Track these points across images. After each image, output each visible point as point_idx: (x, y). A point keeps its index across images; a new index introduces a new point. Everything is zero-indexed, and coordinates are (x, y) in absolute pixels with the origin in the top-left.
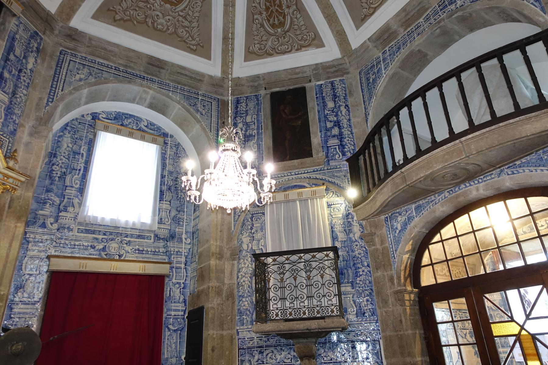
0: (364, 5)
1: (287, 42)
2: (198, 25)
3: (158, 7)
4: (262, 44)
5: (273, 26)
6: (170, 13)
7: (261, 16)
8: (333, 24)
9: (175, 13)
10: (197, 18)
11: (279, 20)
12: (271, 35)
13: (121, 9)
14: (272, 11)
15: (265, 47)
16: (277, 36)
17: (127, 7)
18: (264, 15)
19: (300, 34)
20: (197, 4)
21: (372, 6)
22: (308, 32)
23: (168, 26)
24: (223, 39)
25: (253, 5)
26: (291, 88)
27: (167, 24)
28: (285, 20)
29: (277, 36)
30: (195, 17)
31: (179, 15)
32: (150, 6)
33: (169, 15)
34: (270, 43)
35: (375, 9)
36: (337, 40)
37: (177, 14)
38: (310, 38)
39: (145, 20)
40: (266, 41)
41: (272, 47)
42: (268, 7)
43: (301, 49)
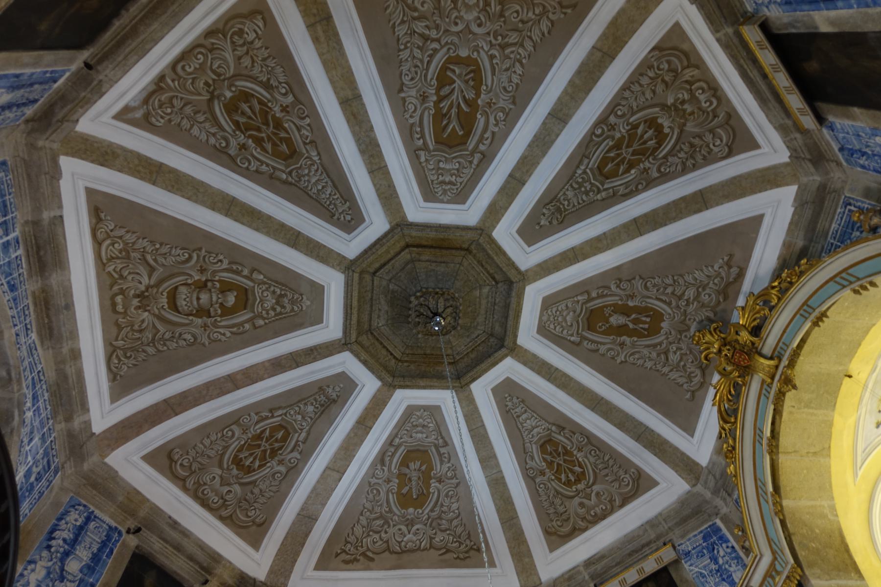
0: (122, 232)
1: (194, 79)
2: (394, 33)
3: (481, 43)
4: (242, 46)
5: (246, 96)
6: (456, 40)
7: (281, 105)
8: (136, 162)
9: (447, 43)
10: (402, 47)
11: (243, 113)
12: (237, 76)
13: (551, 15)
14: (267, 124)
15: (233, 43)
16: (224, 80)
17: (539, 22)
18: (277, 109)
19: (181, 109)
20: (410, 77)
21: (108, 242)
22: (170, 121)
23: (455, 8)
24: (331, 17)
25: (308, 121)
26: (117, 24)
27: (459, 12)
28: (231, 120)
29: (224, 80)
30: (406, 48)
31: (438, 40)
32: (496, 39)
33: (458, 33)
34: (227, 55)
35: (97, 243)
36: (101, 141)
37: (443, 43)
38: (157, 113)
39: (503, 7)
40: (240, 58)
41: (218, 52)
42: (279, 130)
43: (157, 84)
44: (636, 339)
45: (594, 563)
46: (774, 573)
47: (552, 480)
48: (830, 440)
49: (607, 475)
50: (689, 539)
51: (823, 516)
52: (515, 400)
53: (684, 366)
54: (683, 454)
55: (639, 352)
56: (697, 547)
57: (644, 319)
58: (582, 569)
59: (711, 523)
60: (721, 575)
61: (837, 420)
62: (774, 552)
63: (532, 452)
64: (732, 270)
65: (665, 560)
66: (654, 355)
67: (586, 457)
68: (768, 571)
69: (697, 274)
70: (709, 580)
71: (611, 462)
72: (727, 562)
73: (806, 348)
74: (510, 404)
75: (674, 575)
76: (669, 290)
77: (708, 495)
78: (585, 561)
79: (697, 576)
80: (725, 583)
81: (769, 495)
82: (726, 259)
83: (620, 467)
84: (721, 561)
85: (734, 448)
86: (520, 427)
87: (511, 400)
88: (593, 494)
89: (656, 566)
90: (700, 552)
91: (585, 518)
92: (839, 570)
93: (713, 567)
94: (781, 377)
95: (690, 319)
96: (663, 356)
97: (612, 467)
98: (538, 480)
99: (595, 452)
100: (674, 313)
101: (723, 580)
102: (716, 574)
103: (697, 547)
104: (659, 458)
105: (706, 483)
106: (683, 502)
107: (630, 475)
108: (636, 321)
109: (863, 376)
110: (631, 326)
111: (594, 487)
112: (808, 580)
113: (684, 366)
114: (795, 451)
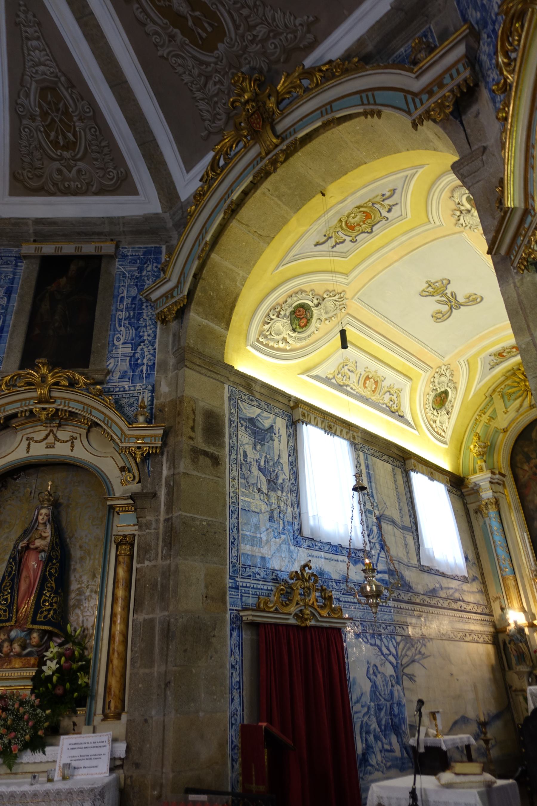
44: (187, 41)
45: (44, 224)
46: (169, 296)
47: (40, 131)
48: (277, 233)
49: (96, 160)
50: (134, 248)
51: (234, 280)
52: (30, 16)
53: (216, 103)
54: (172, 182)
55: (184, 58)
56: (135, 255)
57: (206, 25)
58: (30, 222)
59: (158, 246)
60: (137, 282)
61: (293, 221)
62: (179, 282)
63: (29, 89)
64: (308, 36)
65: (103, 251)
66: (196, 72)
67: (84, 131)
68: (167, 292)
69: (279, 15)
70: (126, 281)
71: (106, 150)
72: (147, 276)
73: (309, 147)
74: (22, 16)
75: (103, 265)
76: (245, 12)
77: (170, 224)
78: (37, 219)
79: (120, 275)
80: (136, 288)
81: (204, 242)
82: (311, 19)
83: (112, 160)
84: (144, 273)
85: (204, 195)
86: (26, 52)
87: (26, 12)
88: (75, 169)
89: (94, 251)
90: (134, 260)
91: (57, 184)
92: (216, 317)
93: (136, 274)
94: (273, 156)
95: (246, 59)
96: (203, 79)
97: (105, 155)
98: (25, 122)
99: (95, 132)
100: (236, 39)
101: (137, 286)
102: (134, 279)
103: (135, 255)
104: (151, 173)
105: (174, 214)
106: (147, 219)
107: (118, 172)
108: (197, 21)
109: (333, 201)
110: (190, 23)
111: (79, 163)
112: (190, 311)
113: (216, 103)
114: (247, 225)
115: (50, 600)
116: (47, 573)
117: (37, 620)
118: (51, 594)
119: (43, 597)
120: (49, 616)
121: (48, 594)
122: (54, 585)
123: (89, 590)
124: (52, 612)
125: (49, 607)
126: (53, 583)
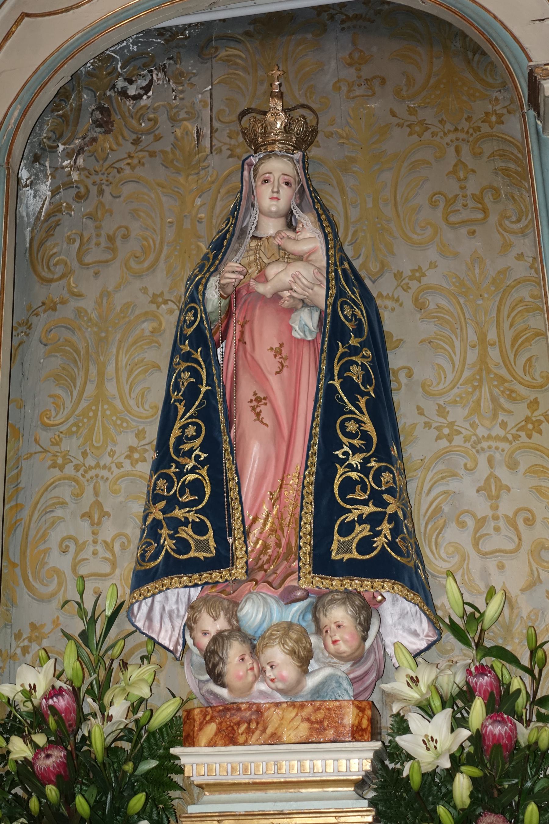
115: (370, 482)
116: (337, 383)
117: (335, 556)
118: (366, 460)
119: (340, 470)
120: (379, 542)
121: (355, 460)
122: (369, 427)
123: (482, 459)
124: (386, 527)
125: (371, 508)
126: (365, 418)
